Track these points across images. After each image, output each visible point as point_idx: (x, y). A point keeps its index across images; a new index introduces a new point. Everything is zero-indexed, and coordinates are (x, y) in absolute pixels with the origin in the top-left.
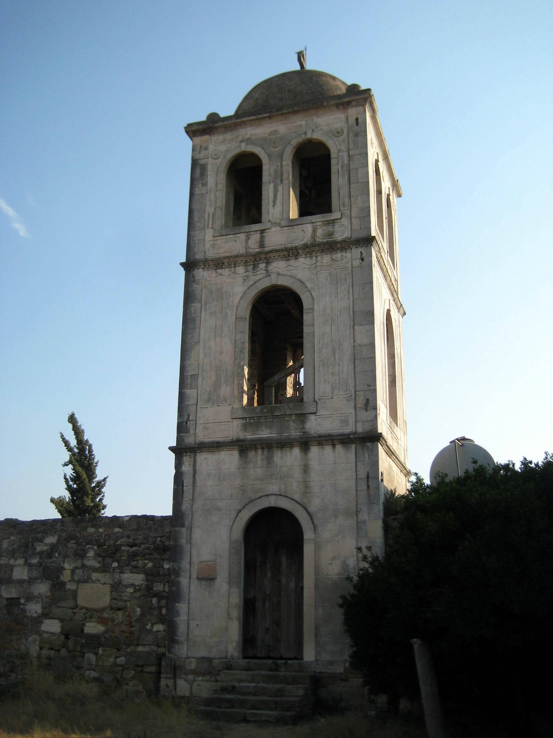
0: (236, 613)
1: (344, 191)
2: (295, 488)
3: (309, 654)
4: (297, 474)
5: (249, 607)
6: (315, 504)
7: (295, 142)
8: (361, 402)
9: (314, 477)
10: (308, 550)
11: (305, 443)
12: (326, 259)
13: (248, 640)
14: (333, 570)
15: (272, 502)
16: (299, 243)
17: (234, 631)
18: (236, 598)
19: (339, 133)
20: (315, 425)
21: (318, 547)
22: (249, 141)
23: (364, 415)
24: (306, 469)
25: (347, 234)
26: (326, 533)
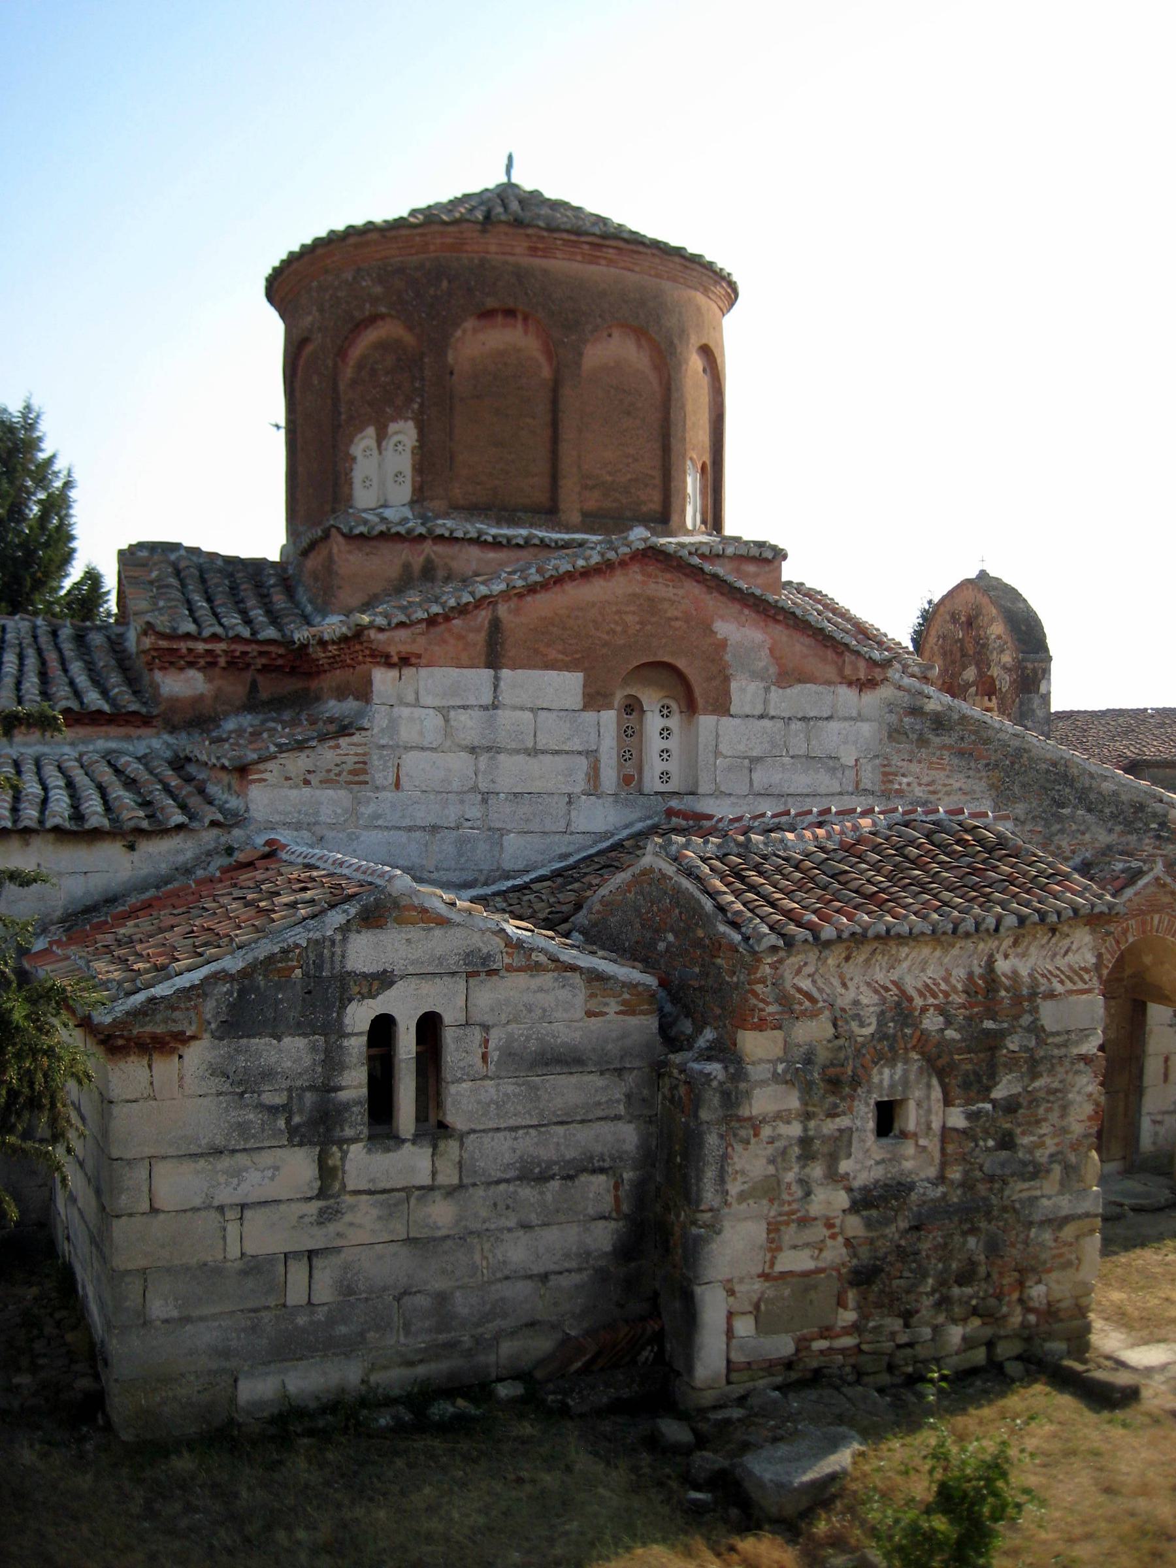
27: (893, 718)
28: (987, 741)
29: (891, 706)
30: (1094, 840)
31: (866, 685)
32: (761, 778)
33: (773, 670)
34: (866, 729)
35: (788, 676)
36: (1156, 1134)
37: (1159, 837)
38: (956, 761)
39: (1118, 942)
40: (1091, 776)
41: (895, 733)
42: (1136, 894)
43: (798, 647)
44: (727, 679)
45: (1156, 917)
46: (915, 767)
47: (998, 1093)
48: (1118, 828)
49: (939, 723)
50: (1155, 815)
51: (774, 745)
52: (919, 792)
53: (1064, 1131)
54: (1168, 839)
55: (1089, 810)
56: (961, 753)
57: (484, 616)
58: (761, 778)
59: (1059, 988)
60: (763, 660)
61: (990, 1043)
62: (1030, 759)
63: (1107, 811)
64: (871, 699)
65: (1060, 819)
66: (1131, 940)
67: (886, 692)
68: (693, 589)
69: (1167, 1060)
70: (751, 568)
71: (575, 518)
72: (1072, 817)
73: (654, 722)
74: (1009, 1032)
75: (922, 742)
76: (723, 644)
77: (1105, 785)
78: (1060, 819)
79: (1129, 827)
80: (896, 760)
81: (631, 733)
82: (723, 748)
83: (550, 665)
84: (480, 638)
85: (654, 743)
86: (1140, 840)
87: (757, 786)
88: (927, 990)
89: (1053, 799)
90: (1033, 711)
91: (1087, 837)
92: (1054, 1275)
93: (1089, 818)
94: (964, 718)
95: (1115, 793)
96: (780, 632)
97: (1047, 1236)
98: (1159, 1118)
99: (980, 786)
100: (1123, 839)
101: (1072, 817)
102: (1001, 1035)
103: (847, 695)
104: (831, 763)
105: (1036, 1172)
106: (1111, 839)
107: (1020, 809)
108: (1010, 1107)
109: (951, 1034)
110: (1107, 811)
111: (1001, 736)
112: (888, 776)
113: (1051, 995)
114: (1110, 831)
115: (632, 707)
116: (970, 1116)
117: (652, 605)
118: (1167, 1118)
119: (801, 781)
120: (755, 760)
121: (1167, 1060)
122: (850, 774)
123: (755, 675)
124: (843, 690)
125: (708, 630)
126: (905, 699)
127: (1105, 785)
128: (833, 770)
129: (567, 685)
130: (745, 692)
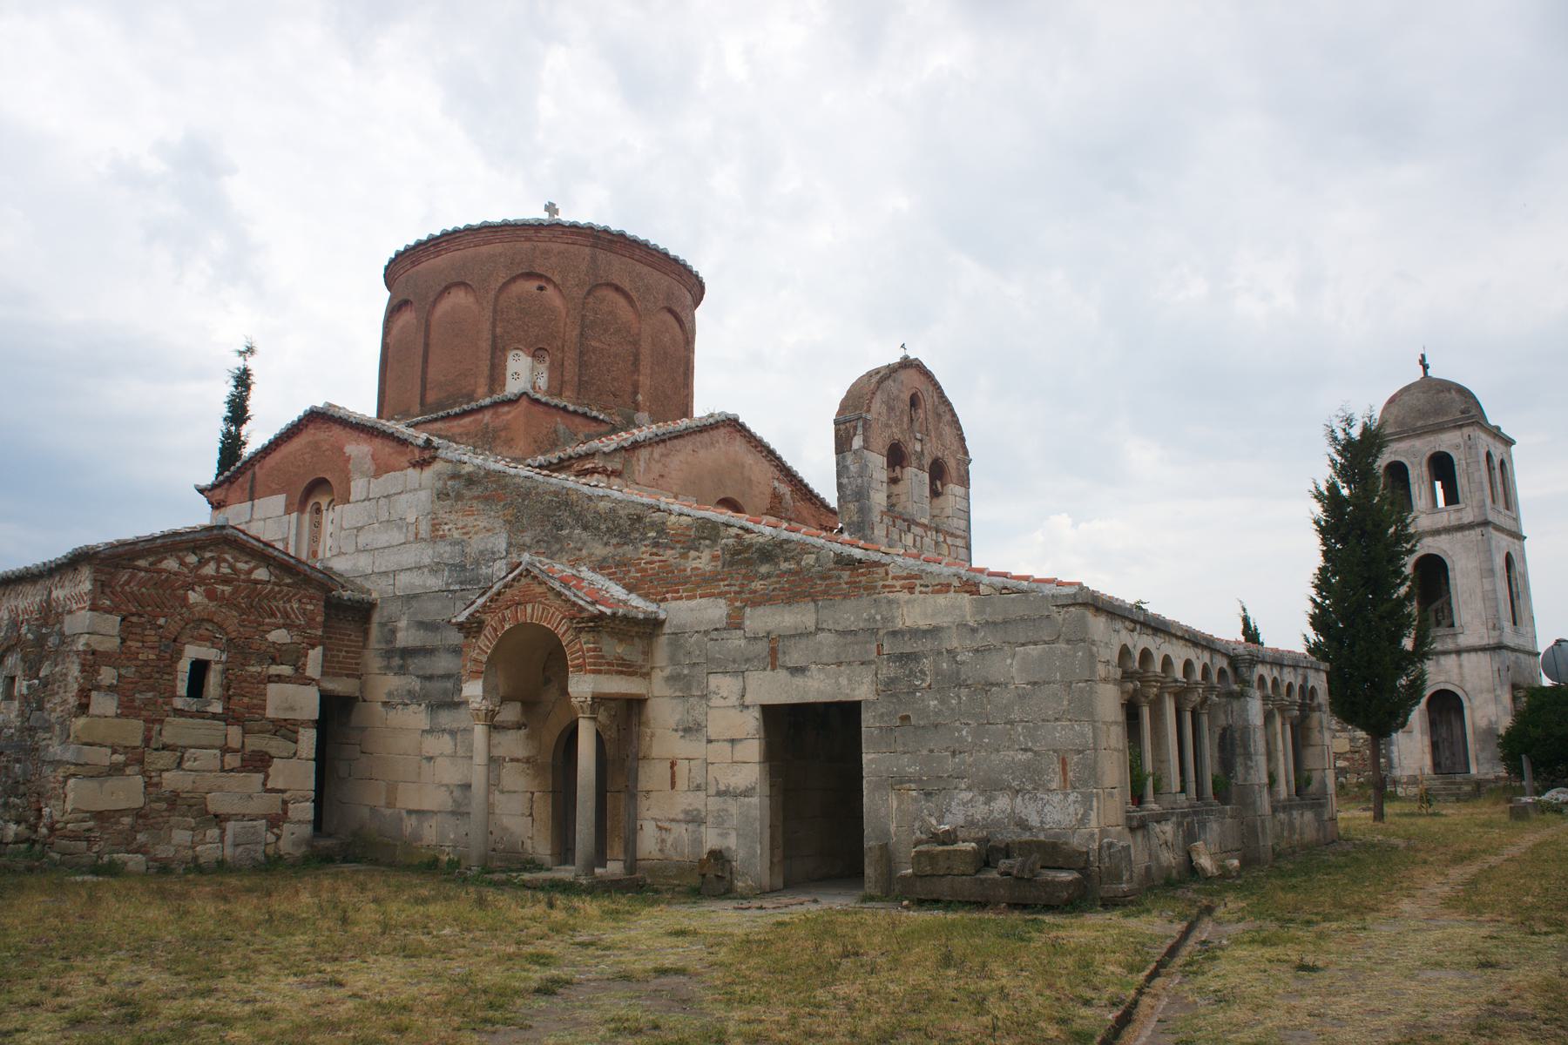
0: (1427, 750)
1: (1466, 489)
2: (1455, 677)
3: (1473, 770)
4: (1456, 670)
5: (1435, 746)
6: (1468, 687)
7: (1428, 454)
8: (1490, 625)
9: (1466, 670)
10: (1467, 712)
11: (1459, 652)
12: (1459, 535)
13: (1436, 765)
14: (1483, 723)
15: (1442, 687)
16: (1440, 526)
17: (1427, 761)
18: (1426, 741)
19: (1457, 447)
20: (1464, 641)
21: (1472, 710)
22: (1395, 453)
23: (1497, 633)
24: (1460, 666)
25: (1471, 519)
26: (1477, 702)
27: (439, 484)
28: (506, 486)
29: (439, 475)
30: (590, 555)
31: (422, 464)
32: (362, 540)
33: (373, 468)
34: (424, 495)
35: (381, 469)
36: (663, 841)
37: (656, 544)
38: (481, 507)
39: (495, 630)
40: (590, 498)
41: (442, 495)
42: (505, 586)
43: (387, 449)
44: (349, 481)
45: (529, 610)
46: (453, 517)
47: (42, 674)
48: (614, 541)
49: (471, 480)
50: (653, 525)
51: (370, 517)
52: (456, 534)
53: (64, 702)
54: (667, 547)
55: (585, 528)
56: (486, 499)
57: (249, 474)
58: (362, 540)
59: (74, 607)
60: (368, 465)
61: (41, 640)
62: (537, 494)
63: (603, 527)
64: (428, 473)
65: (558, 539)
66: (507, 627)
67: (438, 466)
68: (337, 430)
69: (673, 765)
70: (506, 409)
71: (417, 408)
72: (569, 537)
73: (328, 517)
74: (50, 635)
75: (459, 497)
76: (349, 458)
77: (602, 505)
78: (558, 539)
79: (625, 538)
80: (441, 514)
81: (317, 525)
82: (345, 525)
83: (274, 493)
84: (248, 486)
85: (328, 527)
86: (636, 549)
87: (360, 546)
88: (25, 611)
89: (554, 524)
90: (847, 468)
91: (584, 552)
92: (53, 802)
93: (585, 535)
94: (488, 473)
95: (612, 510)
96: (378, 442)
97: (47, 770)
98: (666, 825)
99: (498, 524)
100: (620, 551)
101: (569, 537)
102: (44, 637)
103: (412, 473)
104: (401, 523)
105: (48, 728)
106: (609, 550)
107: (527, 538)
108: (45, 683)
109: (30, 636)
110: (603, 527)
111: (517, 480)
112: (435, 527)
113: (70, 612)
114: (607, 544)
115: (318, 511)
116: (29, 687)
117: (316, 446)
118: (674, 826)
119: (383, 539)
120: (359, 529)
121: (673, 765)
122: (412, 529)
123: (364, 474)
124: (411, 470)
125: (341, 449)
126: (449, 468)
127: (602, 505)
128: (400, 528)
129: (279, 501)
130: (358, 487)
